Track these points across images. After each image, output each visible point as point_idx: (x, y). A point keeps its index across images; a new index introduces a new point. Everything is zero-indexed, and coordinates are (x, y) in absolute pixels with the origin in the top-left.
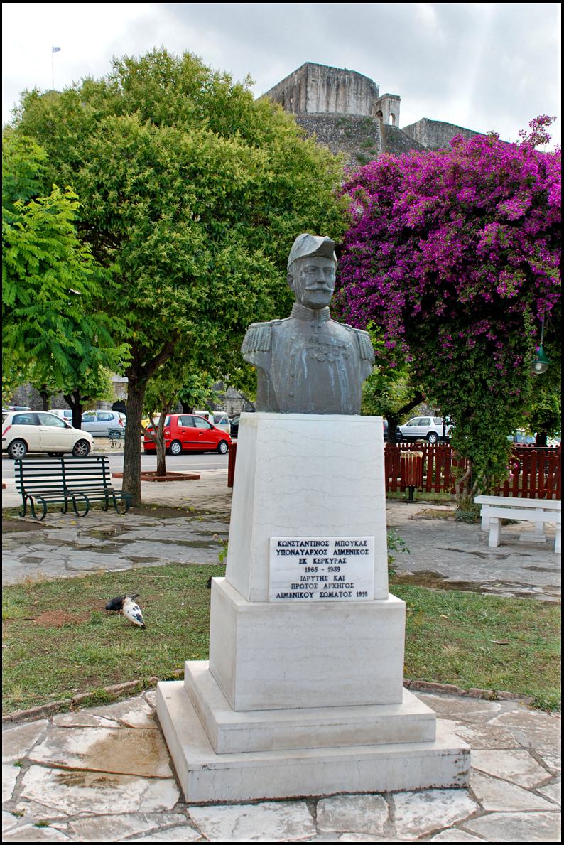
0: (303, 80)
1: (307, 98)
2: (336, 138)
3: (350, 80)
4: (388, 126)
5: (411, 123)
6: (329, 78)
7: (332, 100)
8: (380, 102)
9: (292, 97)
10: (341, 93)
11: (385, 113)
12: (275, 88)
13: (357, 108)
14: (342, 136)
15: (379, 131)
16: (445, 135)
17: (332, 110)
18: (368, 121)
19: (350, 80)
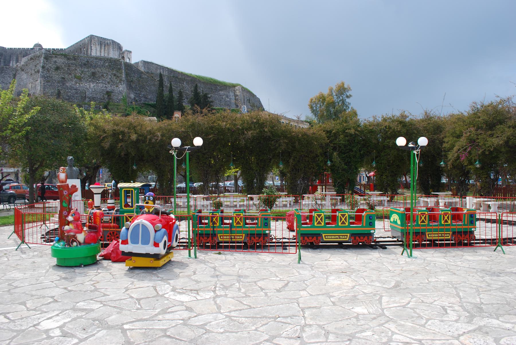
0: (90, 42)
1: (91, 49)
2: (104, 67)
3: (110, 43)
4: (127, 62)
5: (137, 61)
6: (101, 41)
7: (103, 50)
8: (123, 53)
9: (85, 48)
10: (106, 49)
11: (125, 57)
12: (77, 43)
13: (113, 55)
14: (107, 66)
15: (123, 65)
17: (102, 55)
18: (118, 60)
19: (110, 43)
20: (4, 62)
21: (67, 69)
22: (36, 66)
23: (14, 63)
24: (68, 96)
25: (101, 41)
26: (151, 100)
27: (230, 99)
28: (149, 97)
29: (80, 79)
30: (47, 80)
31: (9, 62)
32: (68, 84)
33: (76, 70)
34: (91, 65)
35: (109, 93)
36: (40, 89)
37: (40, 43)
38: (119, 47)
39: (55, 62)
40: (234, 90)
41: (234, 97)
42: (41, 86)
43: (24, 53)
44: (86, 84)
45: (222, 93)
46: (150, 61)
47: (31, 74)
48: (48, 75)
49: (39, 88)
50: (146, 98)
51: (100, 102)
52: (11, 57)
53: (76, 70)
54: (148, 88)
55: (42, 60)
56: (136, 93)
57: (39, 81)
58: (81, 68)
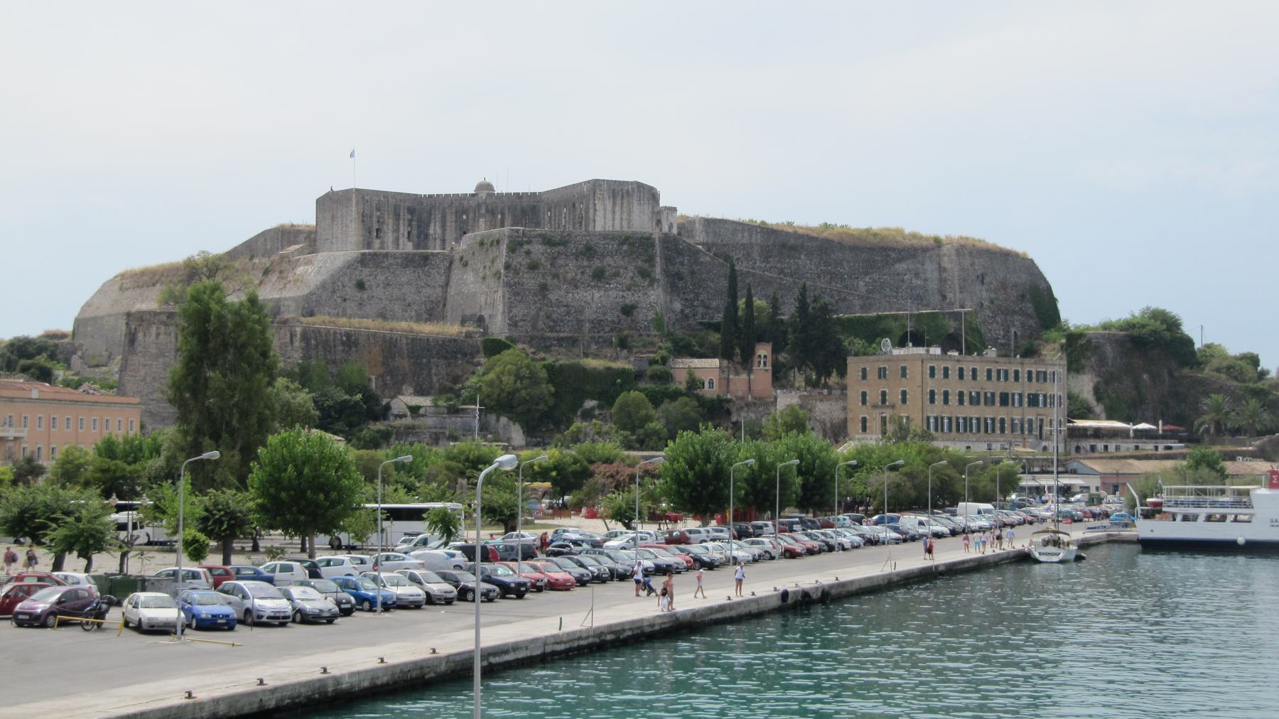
0: (592, 193)
1: (595, 210)
2: (620, 254)
7: (618, 209)
10: (625, 204)
13: (640, 222)
14: (625, 252)
15: (658, 249)
16: (722, 230)
17: (617, 228)
19: (633, 190)
20: (419, 227)
21: (551, 265)
23: (437, 228)
24: (554, 321)
25: (614, 190)
26: (717, 310)
27: (926, 280)
28: (714, 304)
29: (575, 284)
30: (515, 291)
31: (428, 226)
32: (552, 297)
33: (567, 265)
35: (628, 310)
36: (504, 311)
37: (488, 180)
38: (651, 195)
40: (938, 256)
41: (936, 274)
42: (504, 303)
43: (457, 204)
44: (585, 294)
45: (901, 267)
46: (719, 217)
47: (484, 278)
48: (516, 280)
49: (501, 308)
50: (708, 308)
51: (612, 330)
52: (431, 214)
53: (567, 265)
54: (711, 284)
55: (504, 247)
56: (687, 299)
57: (500, 294)
58: (577, 260)
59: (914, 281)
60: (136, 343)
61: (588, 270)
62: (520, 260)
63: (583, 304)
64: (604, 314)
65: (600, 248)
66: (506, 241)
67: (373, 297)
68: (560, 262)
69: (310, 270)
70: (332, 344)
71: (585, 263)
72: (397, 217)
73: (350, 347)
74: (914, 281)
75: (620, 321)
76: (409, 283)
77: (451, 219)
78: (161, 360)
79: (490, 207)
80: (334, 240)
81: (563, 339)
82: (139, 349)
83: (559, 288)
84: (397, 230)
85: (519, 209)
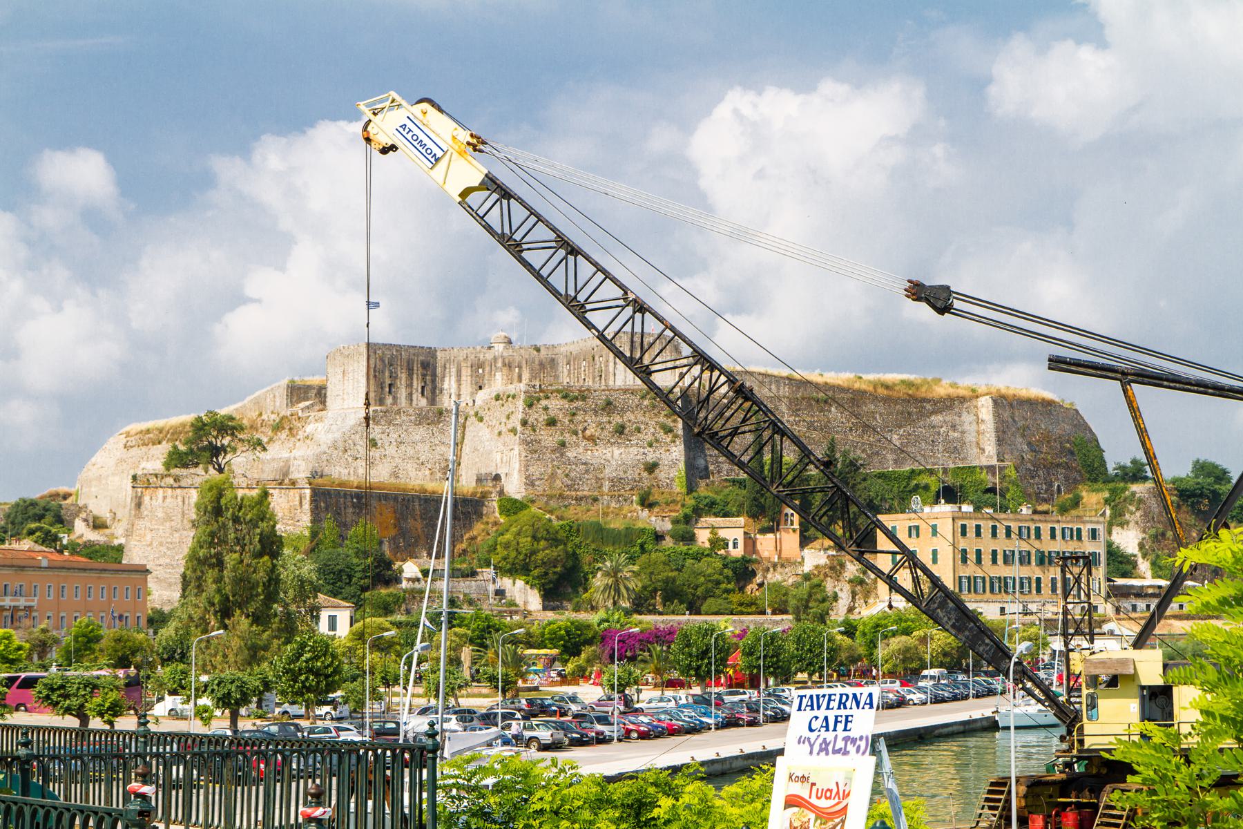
14: (647, 407)
21: (570, 421)
22: (508, 418)
24: (572, 480)
27: (963, 432)
30: (532, 447)
32: (571, 454)
34: (615, 407)
35: (652, 468)
39: (546, 409)
40: (976, 407)
43: (473, 357)
45: (936, 419)
47: (500, 434)
49: (517, 466)
51: (632, 489)
52: (445, 367)
55: (520, 404)
57: (516, 452)
59: (951, 433)
60: (142, 507)
61: (608, 426)
62: (537, 416)
63: (603, 461)
64: (625, 472)
65: (620, 403)
66: (522, 397)
67: (385, 456)
68: (579, 418)
69: (319, 429)
70: (342, 506)
71: (605, 419)
72: (410, 371)
73: (361, 509)
74: (951, 433)
75: (641, 479)
76: (423, 441)
77: (466, 372)
78: (168, 524)
79: (507, 361)
80: (345, 397)
81: (581, 499)
82: (145, 513)
83: (578, 445)
84: (410, 385)
85: (537, 362)
